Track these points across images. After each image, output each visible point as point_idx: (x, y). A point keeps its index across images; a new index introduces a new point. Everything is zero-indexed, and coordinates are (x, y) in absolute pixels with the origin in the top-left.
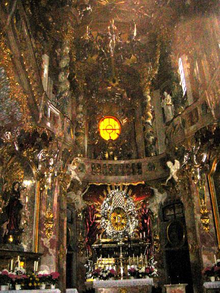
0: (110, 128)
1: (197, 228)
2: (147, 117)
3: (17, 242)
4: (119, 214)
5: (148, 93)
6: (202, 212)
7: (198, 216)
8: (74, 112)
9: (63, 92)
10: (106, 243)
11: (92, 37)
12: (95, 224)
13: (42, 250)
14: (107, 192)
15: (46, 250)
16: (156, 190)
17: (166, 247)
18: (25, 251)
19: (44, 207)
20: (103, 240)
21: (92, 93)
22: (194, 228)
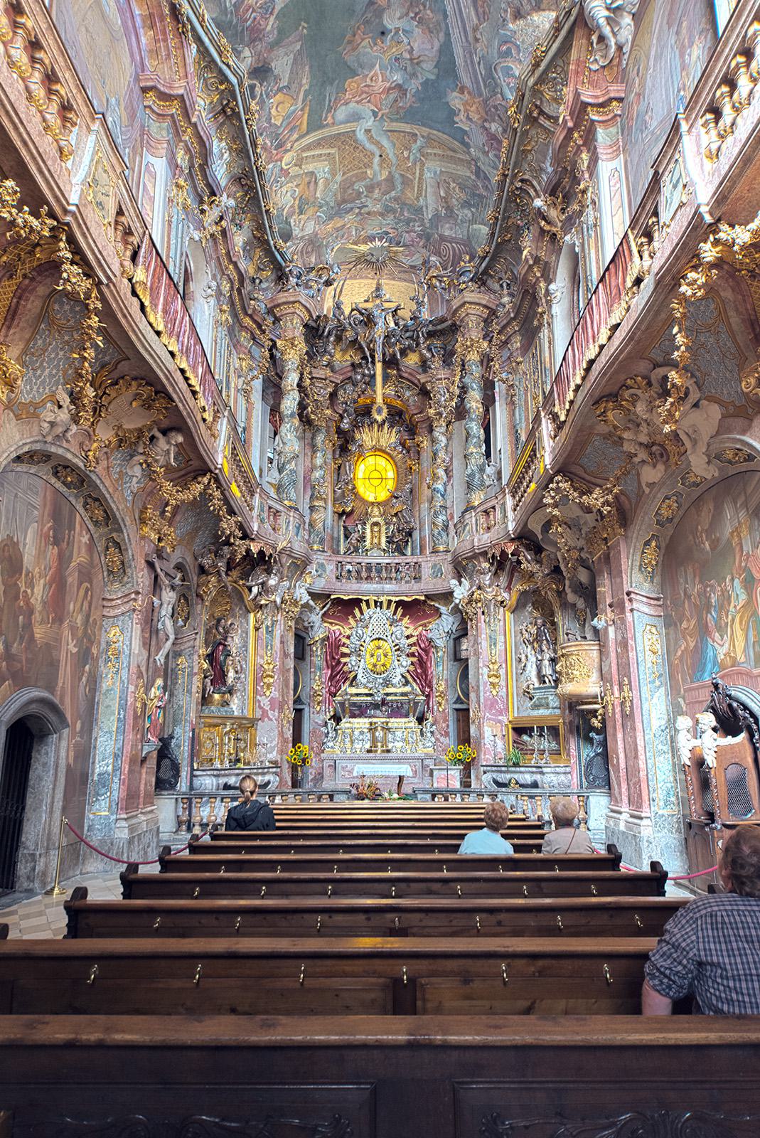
0: (376, 475)
1: (481, 688)
2: (435, 477)
3: (225, 704)
4: (379, 648)
5: (443, 430)
6: (491, 666)
7: (485, 670)
8: (308, 464)
9: (289, 462)
10: (357, 695)
11: (343, 313)
12: (339, 662)
13: (258, 714)
14: (362, 613)
15: (265, 713)
16: (443, 609)
17: (455, 703)
18: (236, 713)
19: (261, 652)
20: (353, 690)
21: (342, 417)
22: (478, 687)
